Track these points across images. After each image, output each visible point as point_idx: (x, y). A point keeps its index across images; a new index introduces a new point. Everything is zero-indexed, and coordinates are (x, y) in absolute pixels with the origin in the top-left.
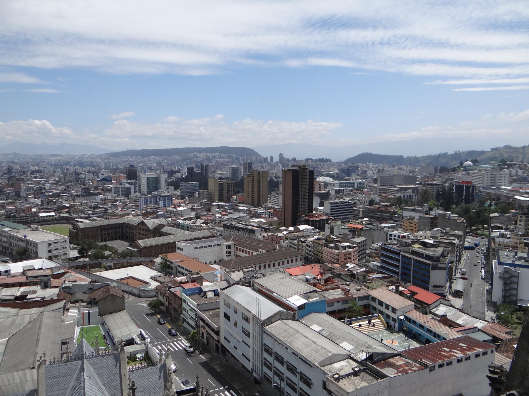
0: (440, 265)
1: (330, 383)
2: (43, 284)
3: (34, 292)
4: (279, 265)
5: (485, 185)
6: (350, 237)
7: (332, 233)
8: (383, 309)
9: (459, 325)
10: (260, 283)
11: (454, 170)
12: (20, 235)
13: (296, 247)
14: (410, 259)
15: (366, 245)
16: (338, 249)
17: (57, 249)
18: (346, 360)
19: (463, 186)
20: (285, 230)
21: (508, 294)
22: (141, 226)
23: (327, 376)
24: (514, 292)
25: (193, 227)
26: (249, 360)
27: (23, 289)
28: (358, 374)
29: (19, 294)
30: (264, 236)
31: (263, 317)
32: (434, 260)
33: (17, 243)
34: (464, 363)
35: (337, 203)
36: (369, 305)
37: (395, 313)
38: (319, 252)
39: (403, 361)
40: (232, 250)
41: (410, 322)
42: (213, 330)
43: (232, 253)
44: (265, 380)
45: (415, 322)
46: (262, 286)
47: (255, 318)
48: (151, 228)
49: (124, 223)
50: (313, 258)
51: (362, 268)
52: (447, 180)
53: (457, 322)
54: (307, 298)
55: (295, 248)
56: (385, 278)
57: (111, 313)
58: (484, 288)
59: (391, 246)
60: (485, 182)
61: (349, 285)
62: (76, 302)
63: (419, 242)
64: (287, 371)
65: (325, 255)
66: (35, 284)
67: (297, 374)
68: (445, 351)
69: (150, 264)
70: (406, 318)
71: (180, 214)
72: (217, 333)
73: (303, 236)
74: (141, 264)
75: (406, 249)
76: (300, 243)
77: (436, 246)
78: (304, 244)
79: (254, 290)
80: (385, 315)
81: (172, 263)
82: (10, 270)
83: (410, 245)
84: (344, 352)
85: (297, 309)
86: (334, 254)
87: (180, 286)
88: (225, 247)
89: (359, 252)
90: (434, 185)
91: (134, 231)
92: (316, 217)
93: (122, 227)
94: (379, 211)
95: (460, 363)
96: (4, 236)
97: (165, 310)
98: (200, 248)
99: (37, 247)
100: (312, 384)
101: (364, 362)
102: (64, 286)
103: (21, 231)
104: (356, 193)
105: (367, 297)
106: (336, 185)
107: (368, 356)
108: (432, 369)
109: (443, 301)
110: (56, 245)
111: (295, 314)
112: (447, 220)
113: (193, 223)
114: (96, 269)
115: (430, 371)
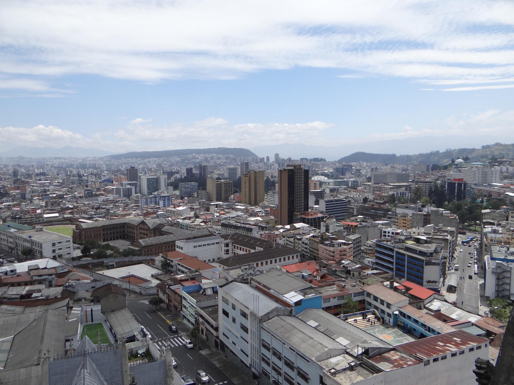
0: (433, 261)
1: (326, 378)
2: (47, 283)
3: (39, 291)
4: (276, 262)
5: (476, 182)
6: (345, 234)
7: (327, 230)
8: (378, 304)
9: (453, 320)
10: (258, 280)
12: (25, 236)
13: (292, 244)
14: (404, 255)
15: (360, 242)
16: (333, 245)
17: (61, 249)
18: (342, 355)
19: (455, 183)
20: (282, 228)
21: (501, 289)
22: (141, 226)
23: (324, 371)
24: (507, 287)
25: (193, 226)
26: (248, 356)
27: (28, 288)
28: (354, 369)
29: (24, 293)
30: (261, 235)
32: (427, 256)
33: (23, 244)
35: (332, 201)
36: (364, 300)
37: (390, 308)
38: (315, 249)
39: (398, 355)
40: (230, 248)
41: (404, 317)
42: (212, 326)
43: (230, 252)
44: (263, 375)
45: (409, 317)
46: (259, 283)
47: (252, 313)
48: (151, 228)
49: (125, 223)
50: (309, 255)
51: (357, 265)
52: (440, 177)
53: (451, 316)
54: (305, 294)
56: (379, 274)
57: (113, 311)
58: (477, 283)
59: (385, 242)
60: (477, 179)
61: (344, 281)
62: (80, 300)
63: (413, 239)
64: (285, 366)
65: (320, 252)
66: (40, 282)
67: (295, 369)
68: (439, 346)
69: (151, 263)
70: (401, 313)
71: (180, 213)
72: (216, 329)
73: (299, 234)
74: (141, 263)
75: (400, 245)
76: (296, 241)
77: (429, 242)
78: (300, 242)
80: (380, 310)
81: (172, 261)
82: (16, 270)
83: (403, 241)
84: (341, 347)
85: (293, 305)
86: (330, 251)
87: (180, 284)
88: (223, 245)
89: (354, 249)
90: (426, 182)
91: (135, 231)
92: (312, 215)
93: (124, 227)
94: (373, 209)
95: (454, 357)
96: (10, 237)
97: (166, 307)
98: (199, 246)
99: (41, 247)
100: (310, 379)
101: (360, 357)
102: (67, 284)
103: (27, 231)
105: (362, 293)
106: (331, 184)
107: (363, 350)
108: (427, 363)
109: (437, 296)
110: (60, 245)
111: (292, 310)
112: (440, 217)
114: (99, 268)
115: (425, 365)
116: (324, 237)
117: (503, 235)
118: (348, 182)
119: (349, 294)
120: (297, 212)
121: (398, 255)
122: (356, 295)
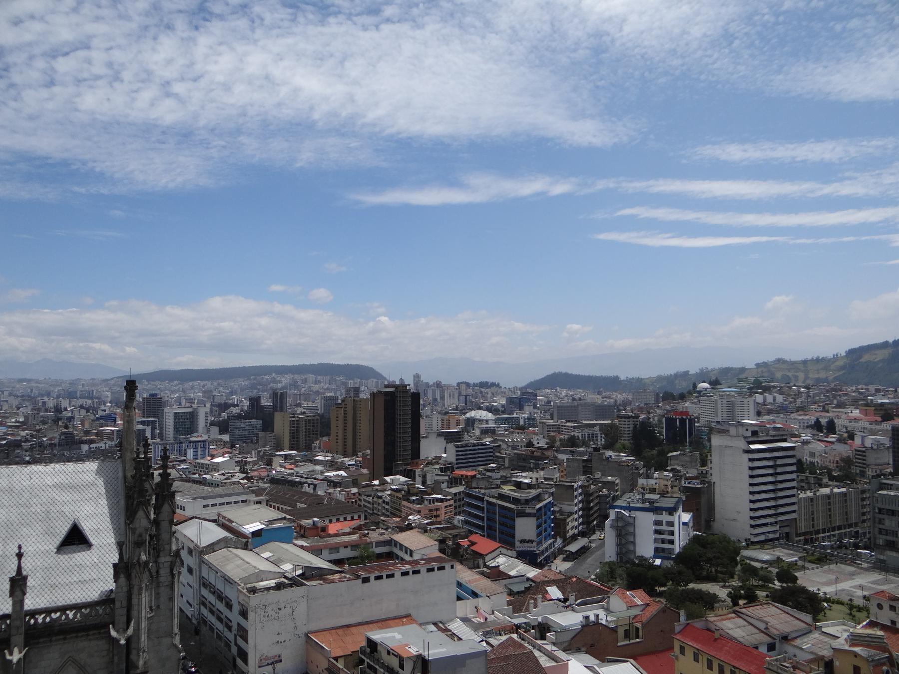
0: (528, 511)
5: (719, 419)
11: (682, 397)
13: (370, 506)
14: (493, 504)
16: (420, 502)
21: (624, 550)
24: (632, 548)
30: (330, 494)
31: (204, 542)
34: (411, 578)
35: (467, 446)
71: (216, 467)
76: (375, 499)
78: (380, 501)
79: (219, 525)
83: (498, 487)
85: (250, 536)
89: (455, 508)
90: (629, 417)
95: (406, 577)
98: (212, 505)
104: (512, 433)
105: (391, 542)
106: (490, 422)
108: (366, 580)
109: (504, 551)
113: (227, 479)
116: (411, 491)
117: (657, 481)
118: (518, 419)
119: (369, 543)
120: (400, 460)
121: (491, 507)
122: (379, 544)
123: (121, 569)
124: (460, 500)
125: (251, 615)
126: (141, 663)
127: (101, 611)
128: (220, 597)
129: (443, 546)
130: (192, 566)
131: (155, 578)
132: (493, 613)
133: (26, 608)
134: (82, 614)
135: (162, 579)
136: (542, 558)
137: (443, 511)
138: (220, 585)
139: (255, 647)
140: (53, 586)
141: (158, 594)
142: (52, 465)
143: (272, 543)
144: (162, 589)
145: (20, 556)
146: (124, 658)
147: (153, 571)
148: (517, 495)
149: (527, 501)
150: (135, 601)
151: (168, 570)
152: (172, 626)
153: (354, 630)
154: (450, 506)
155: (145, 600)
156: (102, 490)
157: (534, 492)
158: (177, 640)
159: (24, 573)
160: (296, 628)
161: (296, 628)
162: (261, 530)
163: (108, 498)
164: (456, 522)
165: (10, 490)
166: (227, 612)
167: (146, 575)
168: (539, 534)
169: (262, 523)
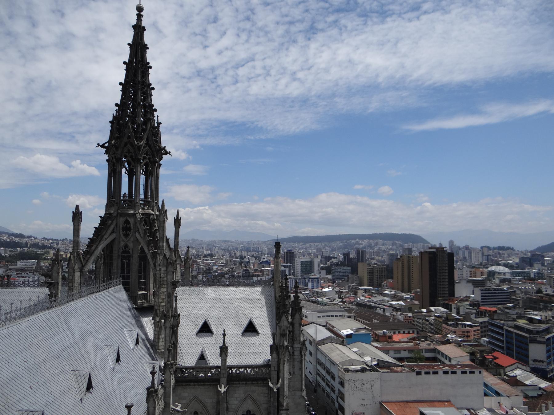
0: (539, 339)
16: (456, 326)
30: (394, 315)
31: (319, 338)
34: (450, 376)
35: (489, 290)
55: (420, 327)
59: (498, 321)
63: (526, 318)
71: (324, 294)
78: (427, 323)
79: (327, 329)
83: (514, 320)
89: (481, 332)
98: (323, 316)
104: (525, 282)
105: (435, 351)
106: (507, 274)
108: (419, 374)
109: (520, 366)
116: (449, 318)
118: (529, 273)
120: (440, 297)
122: (427, 351)
123: (274, 348)
124: (485, 327)
125: (346, 385)
126: (285, 404)
127: (264, 371)
128: (328, 372)
129: (473, 357)
130: (312, 351)
131: (292, 355)
132: (512, 409)
133: (227, 364)
134: (254, 371)
135: (296, 357)
136: (551, 374)
137: (472, 333)
138: (328, 365)
139: (349, 405)
140: (240, 354)
141: (293, 365)
142: (239, 288)
143: (358, 343)
144: (296, 363)
145: (224, 335)
146: (276, 399)
147: (291, 351)
148: (530, 327)
149: (538, 332)
150: (281, 368)
151: (299, 352)
152: (302, 385)
153: (411, 404)
154: (478, 330)
155: (287, 368)
156: (264, 303)
157: (544, 326)
158: (304, 394)
159: (227, 345)
160: (374, 397)
161: (374, 397)
162: (351, 334)
163: (267, 308)
164: (482, 342)
165: (219, 300)
166: (332, 381)
167: (287, 353)
168: (548, 357)
169: (352, 330)
